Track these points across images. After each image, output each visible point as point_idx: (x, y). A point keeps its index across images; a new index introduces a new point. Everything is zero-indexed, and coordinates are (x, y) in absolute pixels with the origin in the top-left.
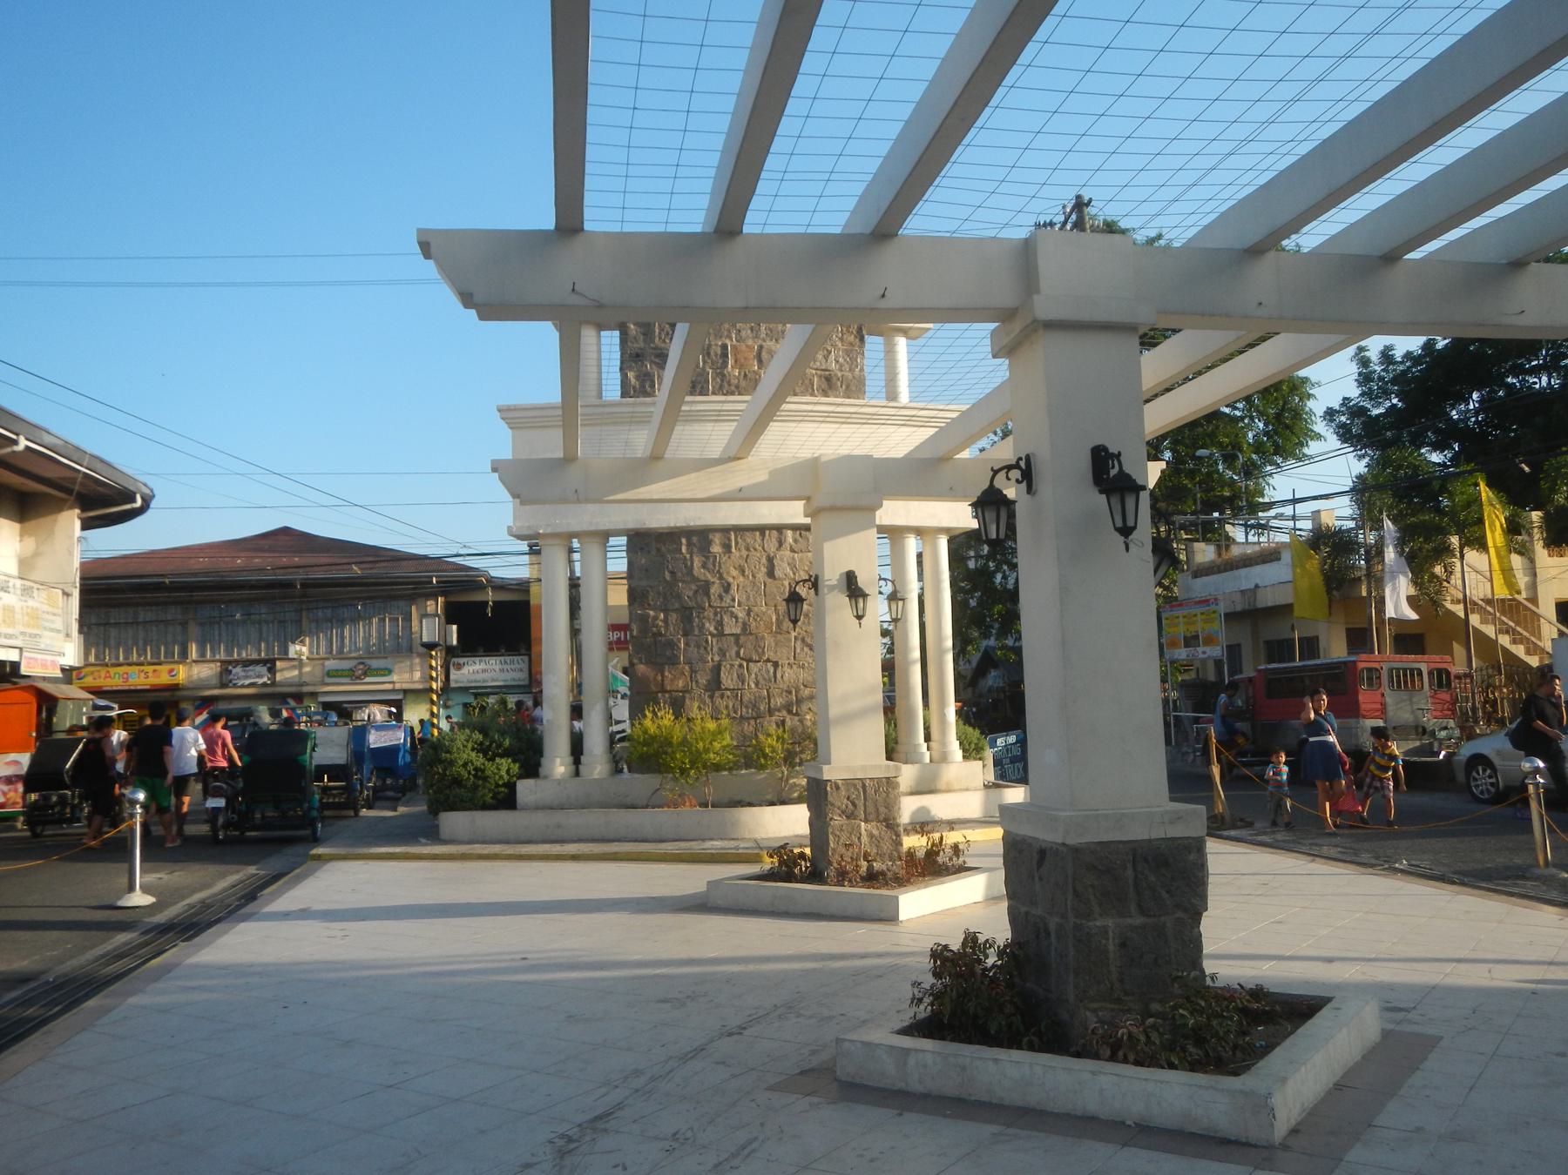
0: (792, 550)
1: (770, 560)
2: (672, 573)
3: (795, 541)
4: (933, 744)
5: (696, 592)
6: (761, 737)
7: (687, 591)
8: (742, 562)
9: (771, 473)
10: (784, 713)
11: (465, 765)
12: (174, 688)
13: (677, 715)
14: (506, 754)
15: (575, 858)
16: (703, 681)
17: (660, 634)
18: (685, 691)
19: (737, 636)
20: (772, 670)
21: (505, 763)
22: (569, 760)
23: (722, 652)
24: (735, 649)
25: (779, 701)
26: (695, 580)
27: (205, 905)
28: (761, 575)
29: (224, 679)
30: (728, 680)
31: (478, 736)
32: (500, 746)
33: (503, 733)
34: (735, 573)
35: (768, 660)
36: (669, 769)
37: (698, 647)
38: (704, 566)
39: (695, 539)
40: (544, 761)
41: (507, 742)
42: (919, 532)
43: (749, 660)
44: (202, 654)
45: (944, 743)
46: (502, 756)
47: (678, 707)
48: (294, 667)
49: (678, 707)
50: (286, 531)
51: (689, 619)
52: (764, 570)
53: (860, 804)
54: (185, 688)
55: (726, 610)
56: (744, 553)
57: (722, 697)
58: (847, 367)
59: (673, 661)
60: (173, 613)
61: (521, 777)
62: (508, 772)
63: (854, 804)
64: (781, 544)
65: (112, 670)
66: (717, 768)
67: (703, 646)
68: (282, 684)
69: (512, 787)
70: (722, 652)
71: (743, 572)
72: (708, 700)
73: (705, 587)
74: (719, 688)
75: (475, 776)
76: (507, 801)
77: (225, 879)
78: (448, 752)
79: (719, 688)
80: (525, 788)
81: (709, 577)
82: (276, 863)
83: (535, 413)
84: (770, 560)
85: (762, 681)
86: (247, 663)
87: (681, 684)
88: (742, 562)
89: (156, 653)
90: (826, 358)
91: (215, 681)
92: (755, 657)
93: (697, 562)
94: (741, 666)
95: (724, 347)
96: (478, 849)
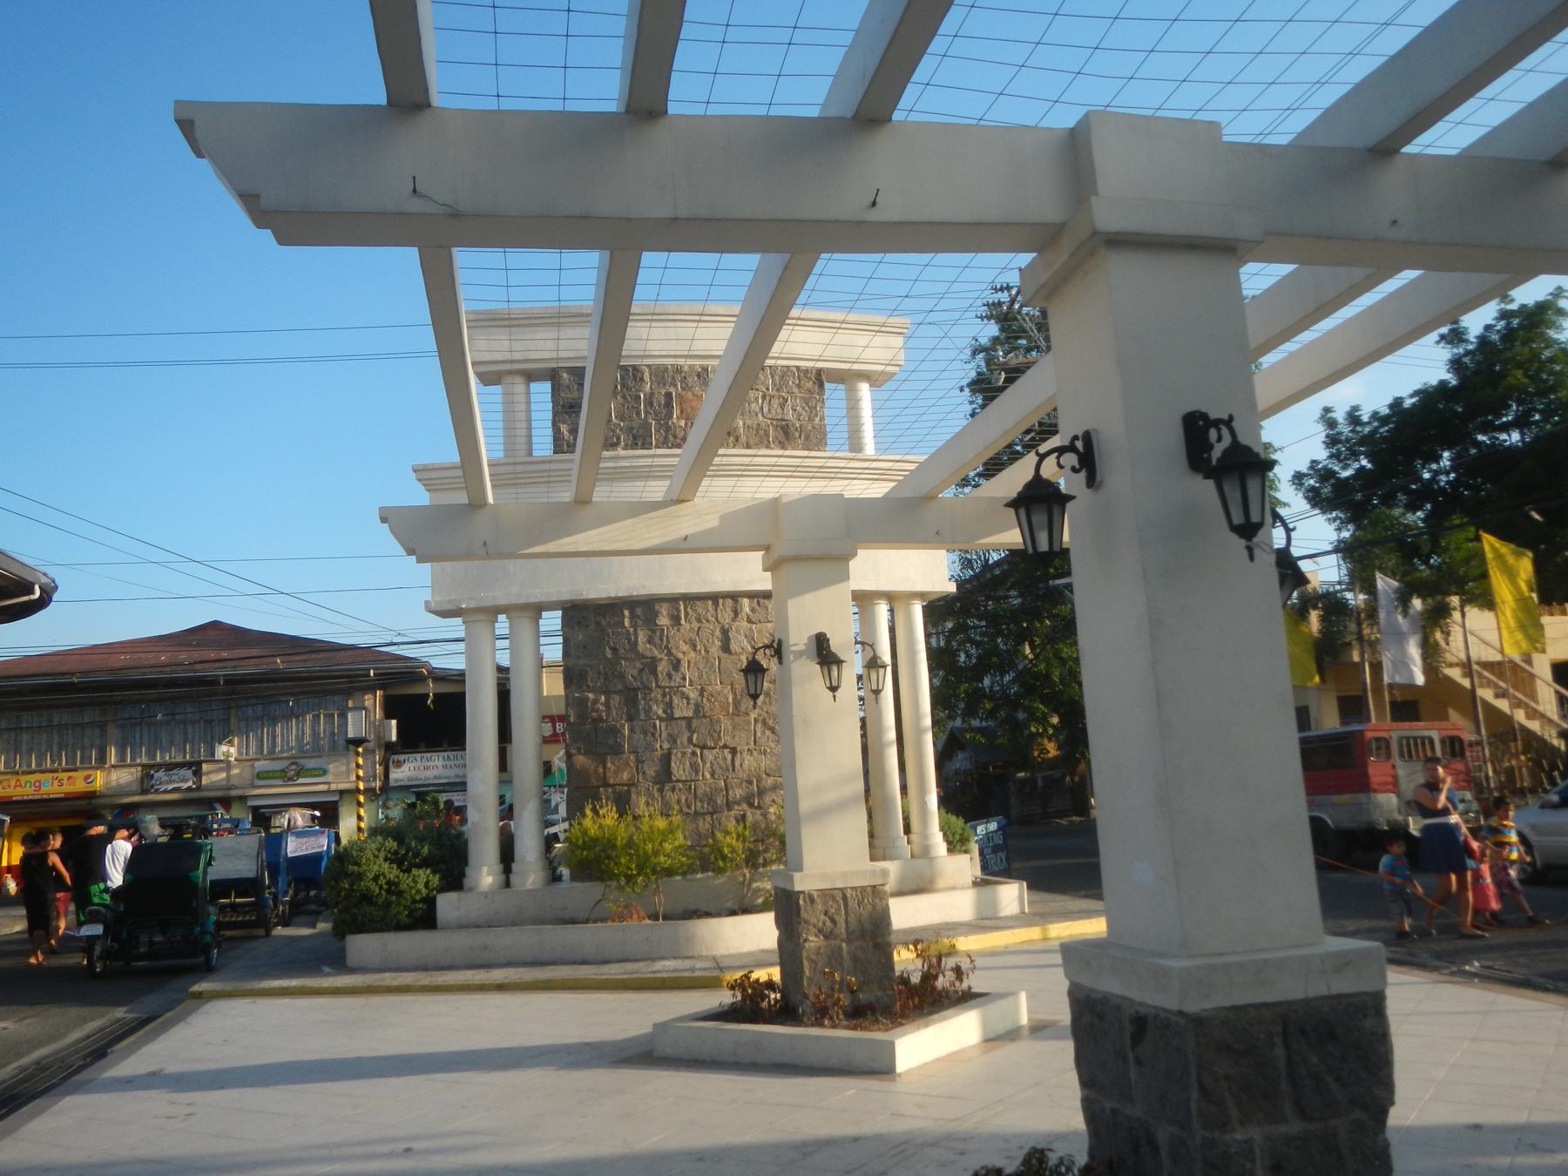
0: (750, 621)
1: (725, 632)
2: (614, 650)
3: (753, 610)
4: (914, 837)
5: (641, 671)
6: (719, 835)
7: (630, 670)
9: (722, 518)
10: (745, 806)
11: (376, 879)
12: (91, 795)
13: (622, 813)
14: (425, 864)
15: (501, 988)
16: (651, 772)
17: (601, 720)
18: (631, 784)
19: (688, 720)
21: (422, 875)
22: (498, 868)
23: (673, 739)
24: (687, 734)
25: (738, 793)
26: (641, 656)
27: (41, 1067)
28: (715, 650)
29: (146, 783)
30: (679, 770)
31: (392, 844)
32: (417, 854)
33: (421, 840)
34: (685, 648)
35: (725, 746)
36: (613, 876)
37: (645, 733)
38: (650, 641)
39: (639, 611)
40: (468, 871)
41: (426, 850)
42: (891, 597)
43: (703, 747)
44: (122, 758)
45: (925, 836)
46: (419, 866)
47: (623, 803)
48: (221, 770)
49: (623, 803)
50: (215, 625)
53: (841, 920)
54: (102, 796)
55: (676, 690)
56: (696, 625)
57: (673, 790)
58: (805, 416)
59: (617, 751)
60: (89, 715)
61: (442, 890)
62: (427, 885)
63: (834, 921)
64: (736, 613)
65: (23, 779)
66: (669, 872)
68: (208, 789)
69: (430, 902)
70: (673, 739)
71: (694, 647)
73: (652, 665)
74: (670, 780)
75: (388, 891)
76: (425, 919)
77: (80, 1024)
78: (359, 865)
79: (670, 780)
80: (447, 904)
81: (656, 652)
82: (152, 1001)
84: (725, 632)
85: (718, 771)
86: (170, 767)
87: (625, 776)
88: (693, 635)
89: (71, 759)
90: (782, 406)
91: (135, 787)
93: (642, 637)
94: (694, 753)
95: (669, 395)
96: (389, 979)
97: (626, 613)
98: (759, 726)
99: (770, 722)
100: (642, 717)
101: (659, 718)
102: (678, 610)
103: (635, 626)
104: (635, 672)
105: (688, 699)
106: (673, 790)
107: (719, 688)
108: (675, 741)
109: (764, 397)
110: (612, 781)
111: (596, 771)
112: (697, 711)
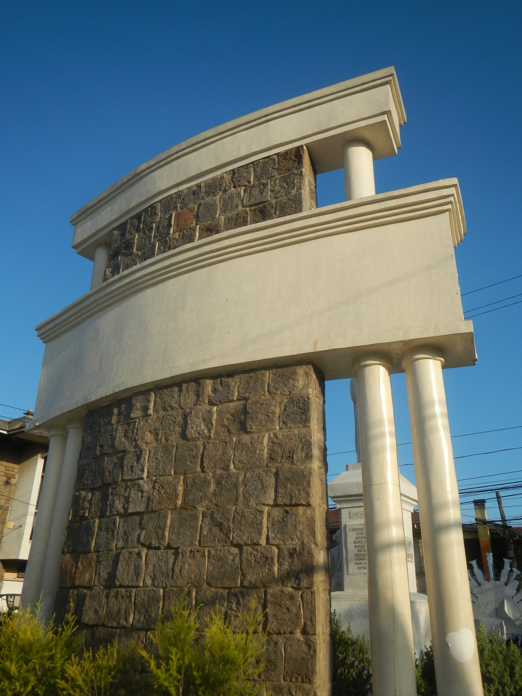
1: (185, 417)
2: (102, 446)
3: (215, 390)
7: (108, 463)
8: (158, 425)
16: (104, 575)
20: (171, 561)
28: (175, 438)
30: (124, 575)
34: (149, 437)
35: (169, 547)
37: (107, 531)
39: (123, 406)
51: (105, 498)
52: (178, 429)
56: (162, 413)
64: (198, 395)
67: (111, 529)
72: (104, 600)
74: (115, 586)
84: (185, 417)
92: (155, 543)
94: (139, 554)
97: (116, 411)
98: (207, 521)
99: (218, 517)
100: (108, 514)
101: (119, 514)
102: (149, 401)
103: (118, 422)
104: (111, 467)
105: (142, 491)
106: (116, 596)
107: (170, 478)
108: (127, 541)
109: (245, 191)
110: (77, 583)
111: (71, 570)
112: (148, 506)
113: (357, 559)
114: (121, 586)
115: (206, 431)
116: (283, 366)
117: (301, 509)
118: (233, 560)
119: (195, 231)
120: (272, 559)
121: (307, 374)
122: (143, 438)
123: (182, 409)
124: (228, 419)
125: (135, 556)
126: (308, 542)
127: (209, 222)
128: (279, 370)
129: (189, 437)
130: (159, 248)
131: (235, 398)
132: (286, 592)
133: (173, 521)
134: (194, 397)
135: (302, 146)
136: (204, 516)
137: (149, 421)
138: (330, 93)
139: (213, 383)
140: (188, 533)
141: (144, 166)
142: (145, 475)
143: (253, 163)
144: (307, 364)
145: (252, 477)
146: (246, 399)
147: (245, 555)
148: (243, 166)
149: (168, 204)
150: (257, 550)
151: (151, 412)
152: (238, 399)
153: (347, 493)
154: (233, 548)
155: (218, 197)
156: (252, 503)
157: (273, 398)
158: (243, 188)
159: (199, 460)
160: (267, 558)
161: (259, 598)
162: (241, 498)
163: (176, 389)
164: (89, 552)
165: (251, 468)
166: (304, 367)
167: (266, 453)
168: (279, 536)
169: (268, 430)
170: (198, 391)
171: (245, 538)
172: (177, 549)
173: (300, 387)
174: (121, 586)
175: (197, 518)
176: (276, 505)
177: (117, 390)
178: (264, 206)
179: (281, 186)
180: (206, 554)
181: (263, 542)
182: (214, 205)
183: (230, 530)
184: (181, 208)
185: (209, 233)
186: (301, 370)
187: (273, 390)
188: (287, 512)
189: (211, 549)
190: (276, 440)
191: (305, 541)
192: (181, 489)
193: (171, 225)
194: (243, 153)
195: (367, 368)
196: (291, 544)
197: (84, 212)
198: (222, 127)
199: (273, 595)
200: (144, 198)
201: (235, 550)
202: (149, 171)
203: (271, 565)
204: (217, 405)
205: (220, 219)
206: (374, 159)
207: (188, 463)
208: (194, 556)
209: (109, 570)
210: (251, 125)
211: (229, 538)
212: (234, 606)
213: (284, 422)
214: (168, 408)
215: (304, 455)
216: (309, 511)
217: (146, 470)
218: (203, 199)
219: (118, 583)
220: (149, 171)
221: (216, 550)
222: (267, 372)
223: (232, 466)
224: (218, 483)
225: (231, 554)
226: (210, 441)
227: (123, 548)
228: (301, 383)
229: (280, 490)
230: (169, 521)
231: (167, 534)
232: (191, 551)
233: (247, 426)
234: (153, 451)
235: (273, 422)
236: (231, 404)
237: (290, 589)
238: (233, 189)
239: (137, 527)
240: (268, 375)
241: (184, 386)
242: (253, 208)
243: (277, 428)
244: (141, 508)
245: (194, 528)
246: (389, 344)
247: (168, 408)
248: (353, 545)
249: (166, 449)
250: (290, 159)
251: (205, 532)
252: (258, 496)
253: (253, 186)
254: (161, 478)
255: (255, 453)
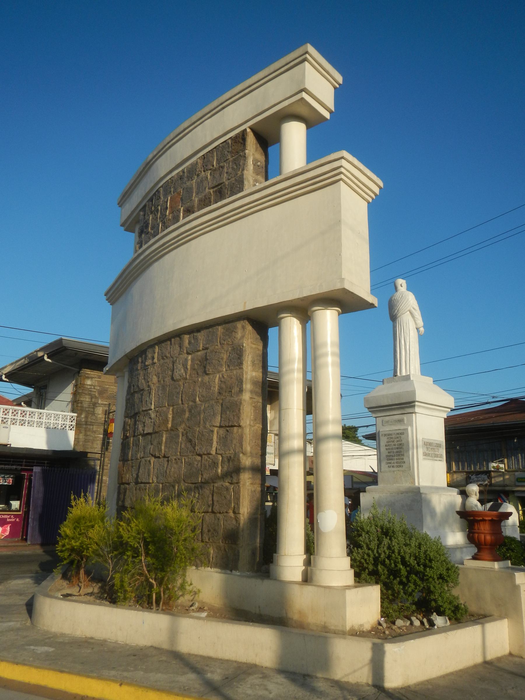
3: (190, 343)
20: (166, 466)
28: (168, 379)
48: (500, 476)
56: (162, 361)
68: (495, 485)
83: (111, 292)
92: (157, 455)
113: (388, 460)
114: (142, 483)
115: (184, 374)
116: (228, 321)
117: (235, 428)
118: (197, 465)
119: (180, 212)
120: (218, 464)
121: (243, 327)
122: (152, 380)
123: (172, 358)
124: (197, 364)
125: (148, 462)
126: (238, 452)
127: (188, 204)
128: (227, 325)
129: (175, 379)
130: (161, 228)
131: (201, 349)
132: (224, 486)
133: (166, 439)
134: (179, 349)
135: (245, 130)
136: (183, 435)
137: (155, 367)
138: (263, 77)
139: (190, 338)
140: (174, 447)
141: (151, 156)
142: (153, 407)
143: (215, 148)
144: (244, 319)
145: (208, 406)
146: (207, 349)
147: (203, 461)
148: (209, 152)
149: (166, 188)
150: (209, 458)
151: (156, 360)
152: (203, 349)
153: (379, 405)
154: (198, 457)
155: (194, 181)
156: (208, 425)
157: (222, 348)
158: (209, 172)
159: (180, 395)
160: (215, 463)
161: (210, 490)
162: (202, 422)
163: (169, 342)
164: (128, 460)
165: (208, 400)
166: (242, 322)
167: (217, 388)
168: (223, 448)
169: (219, 372)
170: (180, 344)
171: (204, 449)
172: (168, 457)
173: (239, 338)
174: (142, 483)
175: (178, 436)
176: (221, 427)
177: (138, 345)
178: (221, 188)
179: (233, 168)
180: (183, 460)
181: (213, 452)
182: (191, 188)
183: (195, 444)
184: (174, 193)
185: (189, 214)
186: (239, 325)
187: (223, 342)
188: (228, 431)
189: (186, 458)
190: (223, 380)
191: (237, 451)
192: (170, 416)
193: (167, 208)
194: (209, 140)
195: (283, 320)
196: (230, 453)
197: (124, 196)
198: (194, 118)
199: (217, 488)
200: (152, 184)
201: (199, 458)
202: (154, 160)
203: (217, 468)
204: (191, 354)
205: (195, 200)
206: (308, 128)
207: (175, 398)
208: (177, 462)
209: (136, 472)
210: (213, 113)
211: (195, 450)
212: (197, 495)
213: (228, 366)
214: (165, 358)
215: (238, 389)
216: (240, 430)
217: (153, 403)
218: (186, 184)
219: (140, 481)
220: (154, 160)
221: (189, 458)
222: (220, 327)
223: (198, 399)
224: (190, 411)
225: (196, 460)
226: (187, 381)
227: (143, 457)
228: (239, 335)
229: (223, 416)
230: (164, 439)
231: (163, 448)
232: (175, 459)
233: (207, 369)
234: (156, 390)
235: (222, 365)
236: (199, 353)
237: (227, 484)
238: (203, 173)
239: (150, 444)
240: (220, 329)
241: (173, 340)
242: (215, 189)
243: (224, 370)
244: (150, 431)
245: (177, 443)
246: (291, 301)
247: (165, 358)
248: (385, 448)
249: (164, 387)
250: (239, 142)
251: (183, 446)
252: (211, 421)
253: (215, 170)
254: (160, 409)
255: (210, 389)
